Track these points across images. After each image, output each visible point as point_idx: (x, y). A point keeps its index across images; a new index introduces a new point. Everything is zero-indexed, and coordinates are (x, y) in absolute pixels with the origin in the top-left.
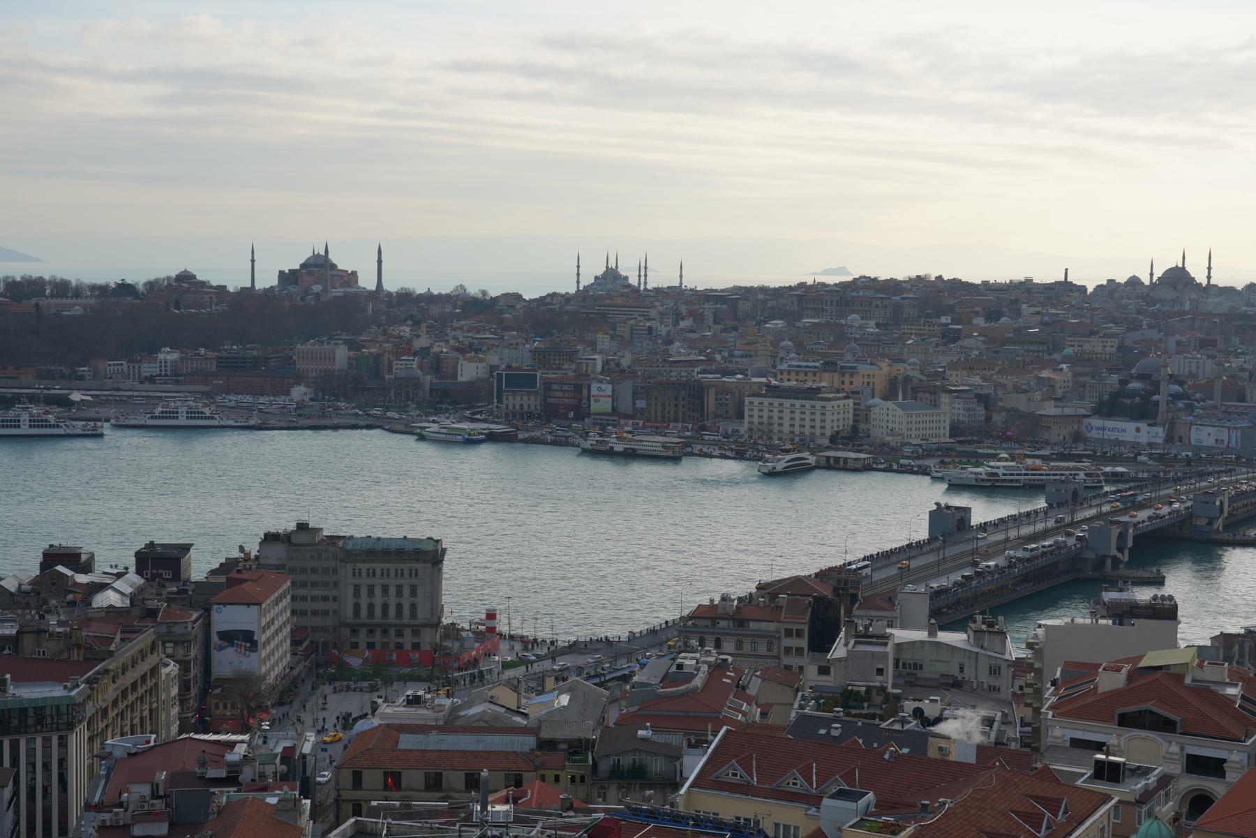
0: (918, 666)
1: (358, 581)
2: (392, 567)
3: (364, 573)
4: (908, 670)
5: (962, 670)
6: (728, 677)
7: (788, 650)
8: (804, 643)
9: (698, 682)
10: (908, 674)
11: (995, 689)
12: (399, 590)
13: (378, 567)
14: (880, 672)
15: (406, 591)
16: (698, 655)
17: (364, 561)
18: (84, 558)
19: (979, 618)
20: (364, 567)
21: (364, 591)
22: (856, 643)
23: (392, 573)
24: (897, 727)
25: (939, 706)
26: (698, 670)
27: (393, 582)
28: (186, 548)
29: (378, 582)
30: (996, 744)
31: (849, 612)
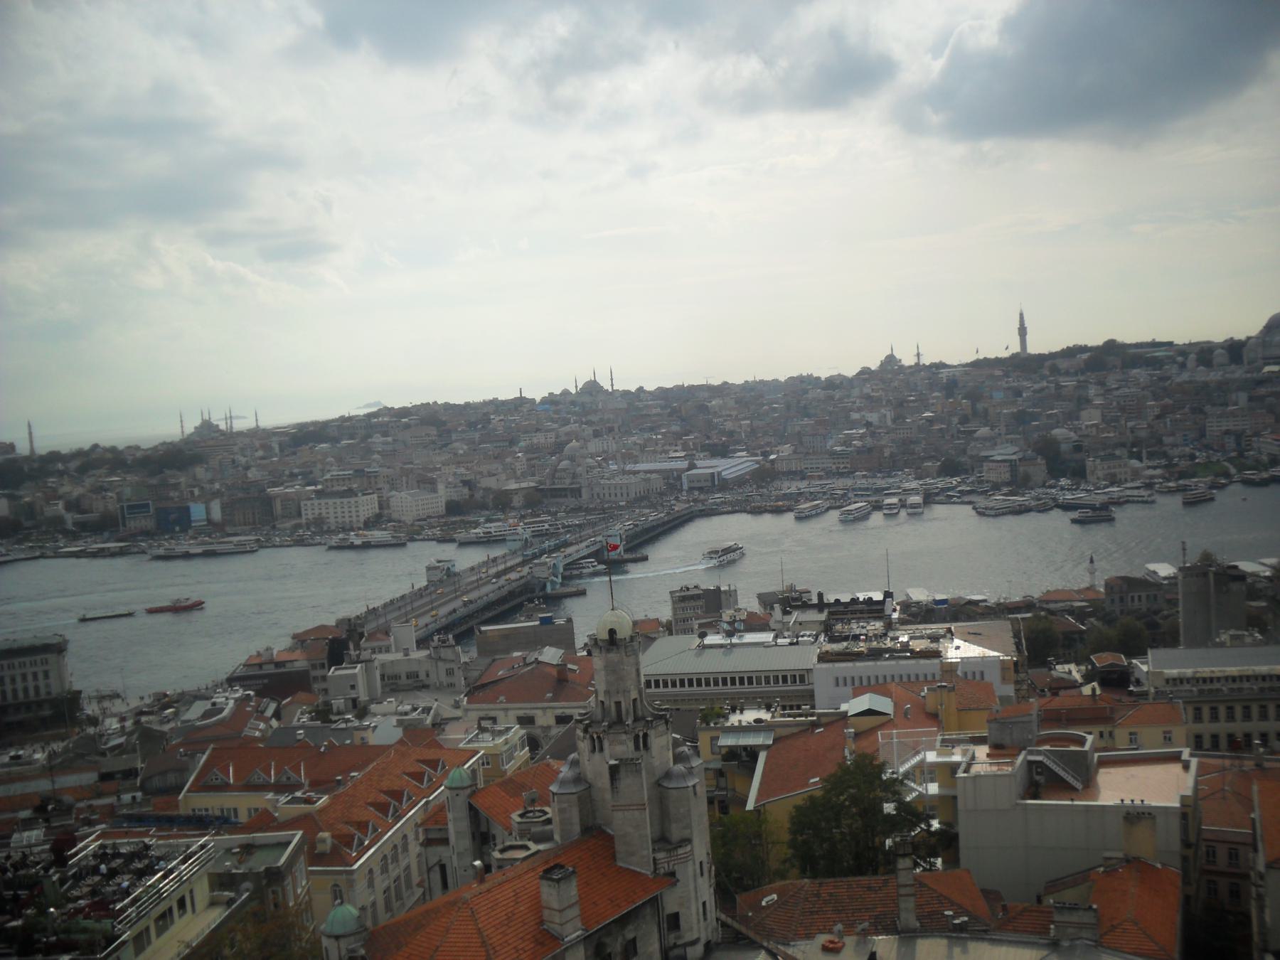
0: (397, 677)
2: (27, 660)
4: (391, 681)
5: (428, 675)
6: (251, 706)
7: (315, 678)
10: (392, 684)
11: (451, 685)
12: (35, 675)
13: (16, 661)
15: (41, 676)
16: (227, 694)
22: (336, 669)
25: (394, 704)
26: (227, 704)
27: (29, 671)
29: (18, 672)
30: (434, 725)
31: (357, 647)
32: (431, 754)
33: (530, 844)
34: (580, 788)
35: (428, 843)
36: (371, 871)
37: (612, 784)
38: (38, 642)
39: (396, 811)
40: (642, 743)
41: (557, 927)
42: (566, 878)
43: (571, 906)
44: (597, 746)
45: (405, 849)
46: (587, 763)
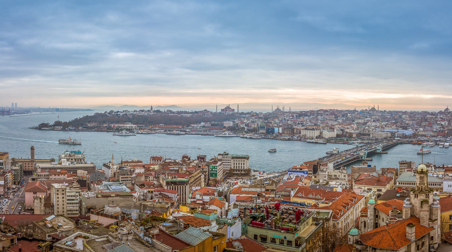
1: (234, 162)
2: (240, 160)
3: (235, 161)
8: (312, 172)
9: (293, 179)
12: (241, 163)
13: (238, 160)
14: (325, 177)
15: (243, 164)
17: (235, 159)
18: (189, 157)
19: (342, 167)
20: (235, 160)
21: (235, 164)
23: (240, 161)
24: (328, 186)
28: (206, 156)
29: (238, 162)
32: (354, 195)
33: (396, 218)
34: (411, 206)
35: (362, 216)
36: (342, 221)
37: (421, 204)
38: (243, 156)
39: (347, 208)
40: (427, 196)
41: (410, 238)
42: (413, 226)
43: (413, 233)
44: (416, 196)
45: (349, 217)
46: (413, 200)
